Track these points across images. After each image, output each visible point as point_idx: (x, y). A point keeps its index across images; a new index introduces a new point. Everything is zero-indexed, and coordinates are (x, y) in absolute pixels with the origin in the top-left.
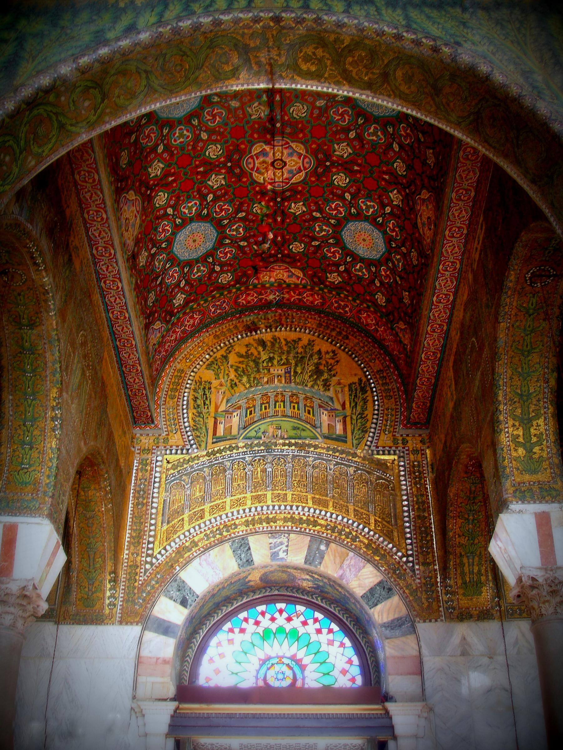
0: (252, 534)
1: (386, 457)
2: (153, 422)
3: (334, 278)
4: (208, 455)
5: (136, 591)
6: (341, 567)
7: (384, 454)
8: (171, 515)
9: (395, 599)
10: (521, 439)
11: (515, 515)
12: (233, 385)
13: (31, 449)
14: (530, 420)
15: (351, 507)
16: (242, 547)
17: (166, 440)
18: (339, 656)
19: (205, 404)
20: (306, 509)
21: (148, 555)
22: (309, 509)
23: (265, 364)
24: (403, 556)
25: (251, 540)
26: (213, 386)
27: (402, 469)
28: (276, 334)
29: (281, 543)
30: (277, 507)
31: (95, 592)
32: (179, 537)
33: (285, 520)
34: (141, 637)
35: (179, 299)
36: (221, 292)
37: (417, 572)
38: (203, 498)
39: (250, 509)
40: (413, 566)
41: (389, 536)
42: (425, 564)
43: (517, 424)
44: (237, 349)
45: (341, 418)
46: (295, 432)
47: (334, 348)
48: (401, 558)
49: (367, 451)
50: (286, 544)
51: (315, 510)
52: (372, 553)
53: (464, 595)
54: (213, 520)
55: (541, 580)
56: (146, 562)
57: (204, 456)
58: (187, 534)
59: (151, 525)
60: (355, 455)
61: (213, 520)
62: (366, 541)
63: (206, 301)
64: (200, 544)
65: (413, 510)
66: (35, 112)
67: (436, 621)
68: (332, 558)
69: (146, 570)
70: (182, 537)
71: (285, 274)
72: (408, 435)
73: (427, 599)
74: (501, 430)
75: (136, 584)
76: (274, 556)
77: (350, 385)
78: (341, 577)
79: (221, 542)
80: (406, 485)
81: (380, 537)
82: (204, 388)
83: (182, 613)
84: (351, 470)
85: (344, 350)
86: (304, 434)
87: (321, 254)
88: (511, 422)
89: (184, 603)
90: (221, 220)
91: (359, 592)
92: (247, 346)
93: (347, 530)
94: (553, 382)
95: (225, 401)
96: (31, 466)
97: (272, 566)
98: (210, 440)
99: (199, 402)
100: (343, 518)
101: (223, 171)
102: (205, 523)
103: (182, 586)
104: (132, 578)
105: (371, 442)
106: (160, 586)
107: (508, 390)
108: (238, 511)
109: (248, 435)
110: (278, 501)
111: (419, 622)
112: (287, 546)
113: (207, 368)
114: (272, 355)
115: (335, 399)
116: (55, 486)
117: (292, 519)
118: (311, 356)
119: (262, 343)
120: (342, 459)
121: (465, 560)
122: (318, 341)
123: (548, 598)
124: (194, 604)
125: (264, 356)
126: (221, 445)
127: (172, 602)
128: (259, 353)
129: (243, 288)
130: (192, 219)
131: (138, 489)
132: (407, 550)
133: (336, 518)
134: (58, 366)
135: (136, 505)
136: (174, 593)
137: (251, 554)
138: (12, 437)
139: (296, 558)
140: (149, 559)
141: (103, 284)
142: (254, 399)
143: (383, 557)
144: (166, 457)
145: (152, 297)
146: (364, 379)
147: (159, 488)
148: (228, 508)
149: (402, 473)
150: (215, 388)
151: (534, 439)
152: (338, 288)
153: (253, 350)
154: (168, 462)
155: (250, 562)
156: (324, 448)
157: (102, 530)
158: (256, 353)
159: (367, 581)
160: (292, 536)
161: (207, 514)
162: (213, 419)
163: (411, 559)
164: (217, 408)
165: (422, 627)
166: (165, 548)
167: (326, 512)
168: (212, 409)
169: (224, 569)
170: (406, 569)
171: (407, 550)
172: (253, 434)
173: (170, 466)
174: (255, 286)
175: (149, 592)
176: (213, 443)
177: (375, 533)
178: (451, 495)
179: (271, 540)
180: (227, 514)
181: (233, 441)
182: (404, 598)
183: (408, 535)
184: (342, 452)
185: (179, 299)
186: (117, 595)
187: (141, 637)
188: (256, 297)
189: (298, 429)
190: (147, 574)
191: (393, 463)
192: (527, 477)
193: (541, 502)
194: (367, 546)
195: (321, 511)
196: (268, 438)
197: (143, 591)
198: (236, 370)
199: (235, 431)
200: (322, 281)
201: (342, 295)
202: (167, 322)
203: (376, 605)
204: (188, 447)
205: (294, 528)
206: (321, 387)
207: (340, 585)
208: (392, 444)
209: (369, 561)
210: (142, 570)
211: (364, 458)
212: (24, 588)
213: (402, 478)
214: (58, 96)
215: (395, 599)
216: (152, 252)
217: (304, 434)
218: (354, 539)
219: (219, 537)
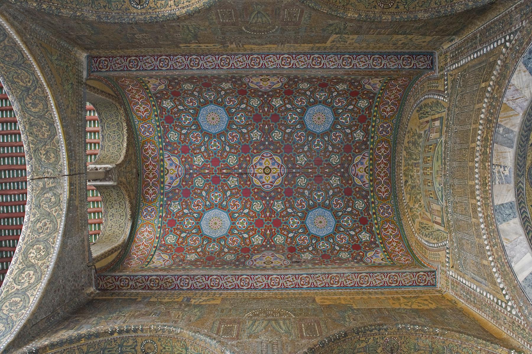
0: (493, 201)
4: (450, 232)
21: (506, 308)
36: (371, 208)
56: (510, 312)
57: (451, 235)
64: (500, 254)
75: (527, 331)
77: (420, 118)
86: (440, 153)
90: (309, 205)
98: (442, 228)
108: (480, 212)
126: (445, 220)
128: (409, 185)
131: (465, 299)
139: (509, 158)
140: (509, 309)
152: (366, 132)
157: (464, 346)
169: (516, 233)
170: (516, 40)
178: (426, 15)
184: (448, 119)
200: (364, 143)
201: (373, 129)
206: (421, 140)
210: (517, 318)
217: (440, 153)
219: (494, 234)
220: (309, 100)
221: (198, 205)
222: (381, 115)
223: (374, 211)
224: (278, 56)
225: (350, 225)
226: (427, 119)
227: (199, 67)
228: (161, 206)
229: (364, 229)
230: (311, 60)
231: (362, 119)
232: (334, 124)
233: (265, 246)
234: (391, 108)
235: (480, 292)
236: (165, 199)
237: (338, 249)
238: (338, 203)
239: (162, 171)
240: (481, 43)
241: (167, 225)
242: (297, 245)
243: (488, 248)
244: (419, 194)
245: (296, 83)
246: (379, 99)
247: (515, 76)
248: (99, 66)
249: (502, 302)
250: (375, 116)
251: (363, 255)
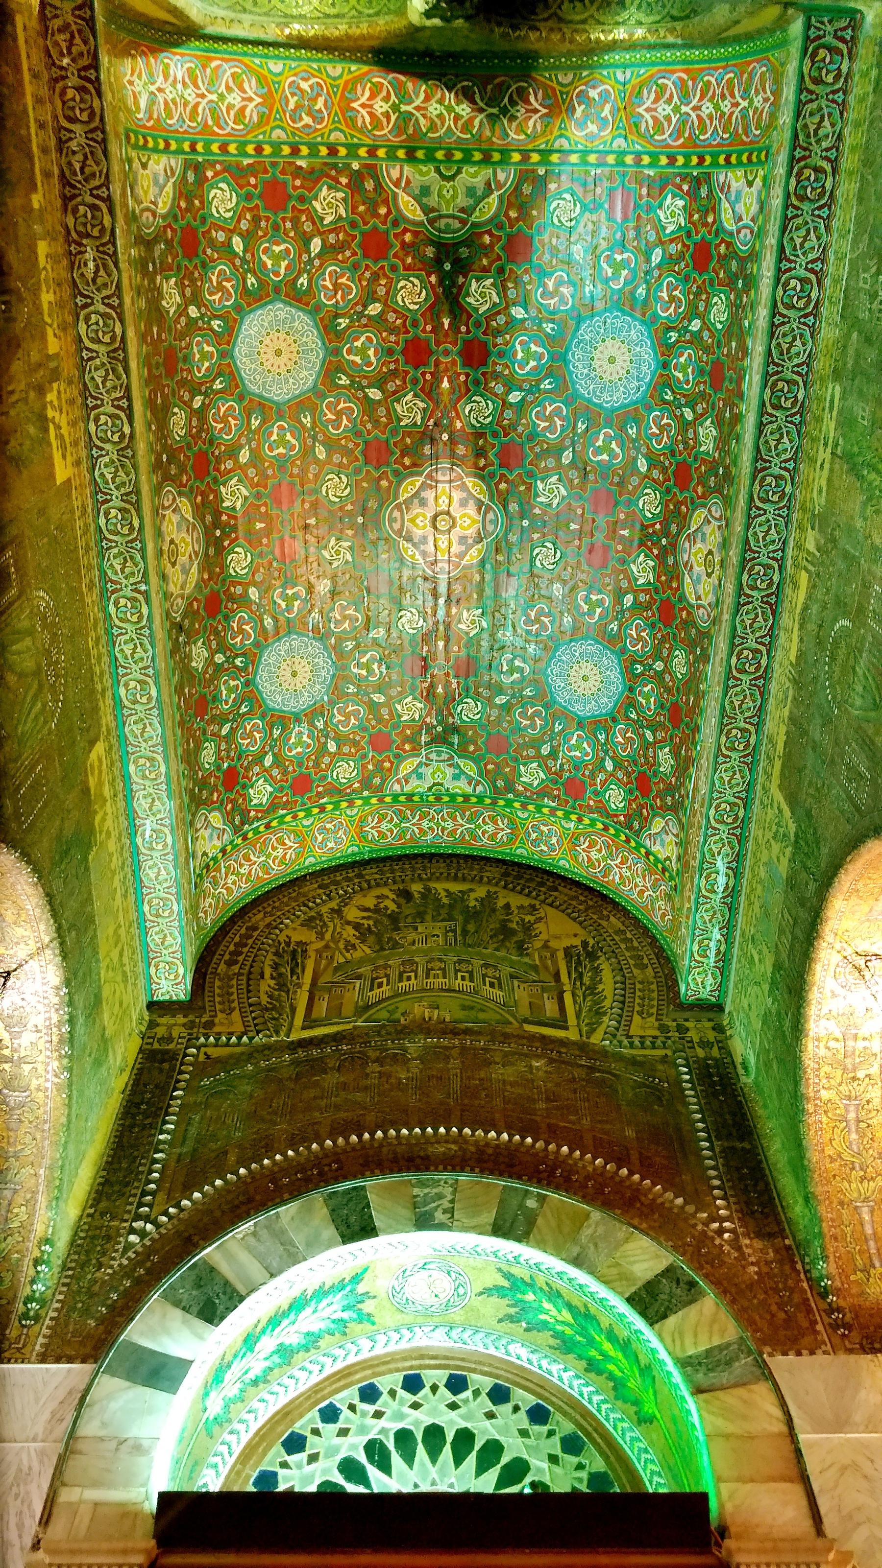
7: (643, 1047)
9: (710, 1302)
19: (293, 972)
29: (440, 1196)
37: (747, 1251)
40: (736, 1239)
45: (555, 994)
46: (466, 1013)
47: (533, 902)
50: (450, 1197)
63: (309, 814)
65: (718, 1138)
67: (812, 1353)
68: (553, 1223)
71: (449, 772)
73: (781, 1306)
81: (654, 1184)
85: (551, 905)
86: (482, 1016)
87: (510, 723)
92: (378, 897)
98: (299, 1020)
111: (771, 1355)
112: (452, 1201)
113: (302, 925)
115: (541, 969)
122: (502, 893)
129: (374, 801)
137: (371, 1217)
141: (112, 609)
142: (386, 966)
165: (781, 1364)
174: (395, 797)
183: (716, 1182)
185: (260, 792)
188: (396, 826)
189: (472, 1008)
198: (357, 926)
202: (236, 830)
203: (665, 1317)
208: (657, 1033)
220: (641, 663)
221: (336, 286)
222: (583, 834)
223: (329, 807)
224: (767, 640)
225: (290, 750)
226: (564, 978)
227: (770, 410)
229: (281, 789)
230: (742, 725)
231: (575, 789)
232: (565, 715)
233: (216, 524)
234: (598, 860)
236: (355, 166)
237: (224, 732)
238: (349, 718)
239: (449, 156)
240: (728, 1153)
241: (267, 176)
242: (226, 617)
245: (690, 645)
246: (623, 838)
248: (824, 46)
250: (580, 820)
251: (213, 803)
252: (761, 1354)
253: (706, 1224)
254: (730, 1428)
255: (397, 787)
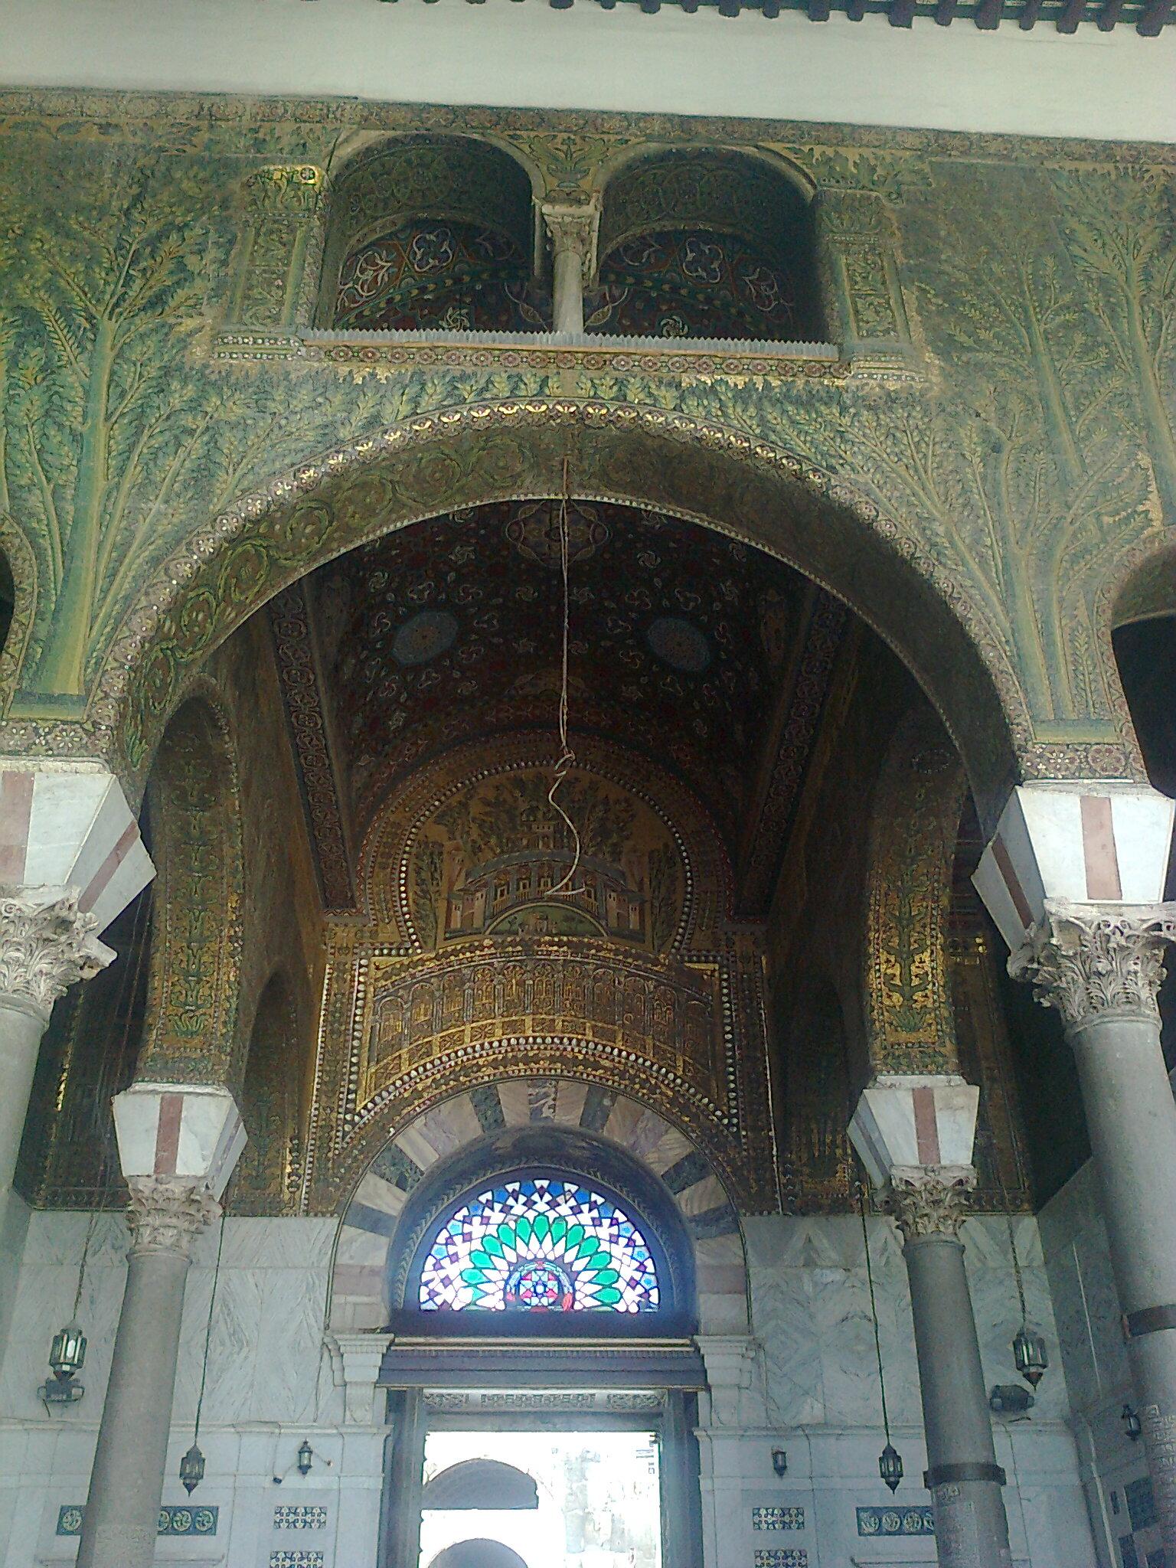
1: (703, 966)
2: (354, 906)
3: (632, 693)
5: (330, 1165)
6: (633, 1132)
8: (383, 1049)
10: (897, 982)
11: (885, 1092)
12: (476, 850)
13: (198, 983)
14: (911, 954)
15: (649, 1041)
16: (487, 1099)
17: (374, 934)
18: (627, 1260)
20: (583, 1044)
22: (588, 1042)
23: (524, 818)
24: (724, 1116)
25: (500, 1087)
26: (445, 850)
27: (725, 984)
28: (541, 769)
29: (546, 1095)
30: (539, 1040)
31: (269, 1166)
32: (394, 1084)
33: (553, 1059)
34: (337, 1235)
35: (397, 719)
38: (429, 1023)
39: (500, 1042)
41: (704, 1087)
42: (756, 1129)
43: (893, 959)
44: (482, 792)
45: (637, 905)
48: (720, 1119)
49: (674, 956)
51: (596, 1045)
52: (677, 1112)
53: (810, 1176)
54: (445, 1059)
55: (917, 1184)
58: (406, 1078)
59: (352, 1064)
60: (656, 962)
61: (445, 1059)
62: (670, 1093)
64: (425, 1095)
66: (240, 550)
69: (345, 1134)
70: (398, 1083)
72: (734, 933)
73: (757, 1181)
74: (870, 967)
75: (330, 1155)
76: (536, 1113)
78: (634, 1146)
79: (457, 1092)
80: (729, 1009)
82: (432, 854)
83: (398, 1199)
84: (651, 985)
86: (580, 928)
88: (883, 957)
89: (401, 1184)
91: (659, 1169)
93: (643, 1076)
94: (945, 901)
95: (463, 874)
96: (198, 1007)
97: (531, 1128)
98: (441, 935)
99: (424, 875)
100: (637, 1058)
101: (473, 541)
102: (432, 1062)
103: (399, 1158)
104: (323, 1144)
105: (681, 942)
106: (366, 1157)
107: (882, 911)
108: (482, 1045)
109: (500, 927)
110: (542, 1030)
114: (534, 804)
115: (628, 874)
116: (234, 1037)
117: (562, 1059)
118: (594, 806)
119: (520, 784)
120: (637, 967)
121: (813, 1126)
123: (927, 1211)
124: (416, 1185)
125: (523, 806)
127: (384, 1182)
128: (516, 800)
130: (422, 608)
131: (331, 1009)
132: (730, 1108)
133: (627, 1058)
134: (239, 863)
135: (328, 1034)
136: (388, 1170)
138: (171, 965)
140: (348, 1117)
142: (506, 872)
143: (694, 1117)
144: (374, 959)
145: (359, 719)
146: (672, 845)
147: (363, 1007)
148: (467, 1040)
149: (725, 991)
150: (449, 853)
151: (916, 982)
153: (506, 795)
154: (377, 968)
155: (500, 1122)
156: (610, 951)
158: (510, 800)
159: (671, 1154)
160: (561, 1083)
161: (436, 1049)
162: (445, 904)
163: (735, 1121)
164: (451, 885)
166: (372, 1101)
167: (613, 1049)
168: (444, 886)
171: (730, 1108)
172: (505, 926)
173: (379, 974)
175: (349, 1168)
176: (446, 939)
177: (684, 1082)
179: (531, 1091)
180: (465, 1050)
181: (475, 937)
182: (723, 1178)
183: (732, 1086)
184: (637, 957)
185: (397, 719)
186: (301, 1172)
187: (337, 1235)
190: (347, 1139)
191: (712, 975)
192: (903, 1036)
193: (921, 1073)
194: (671, 1101)
195: (604, 1046)
196: (528, 933)
197: (341, 1166)
198: (480, 826)
199: (478, 923)
204: (408, 945)
205: (565, 1073)
207: (632, 1159)
209: (674, 1124)
210: (340, 1134)
211: (669, 967)
212: (192, 1190)
213: (725, 999)
214: (271, 526)
215: (712, 1180)
216: (362, 657)
217: (580, 928)
218: (653, 1090)
228: (458, 280)
235: (353, 1048)
243: (429, 1066)
244: (500, 844)
247: (678, 1135)
249: (354, 1101)
252: (737, 1214)
253: (720, 1119)
254: (712, 1262)
255: (513, 692)
